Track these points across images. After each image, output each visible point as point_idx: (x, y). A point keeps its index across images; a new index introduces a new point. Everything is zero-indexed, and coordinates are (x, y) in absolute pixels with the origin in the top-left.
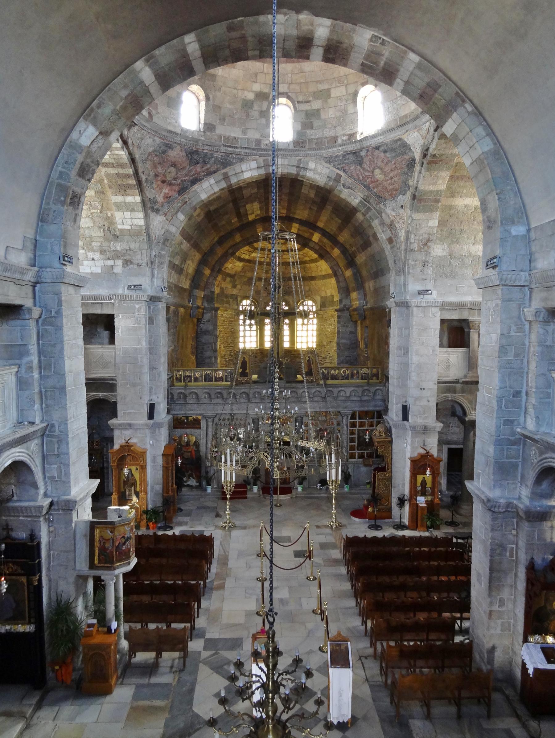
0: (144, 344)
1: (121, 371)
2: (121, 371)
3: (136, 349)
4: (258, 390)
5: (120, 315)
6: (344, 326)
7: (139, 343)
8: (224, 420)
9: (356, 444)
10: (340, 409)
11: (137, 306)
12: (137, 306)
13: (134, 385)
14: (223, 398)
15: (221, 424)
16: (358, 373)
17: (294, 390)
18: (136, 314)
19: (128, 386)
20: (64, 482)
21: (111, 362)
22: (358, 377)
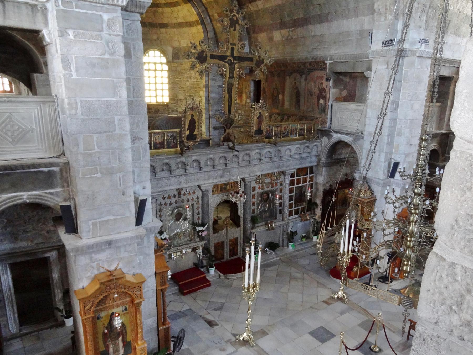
0: (124, 94)
1: (81, 147)
2: (81, 147)
3: (108, 105)
4: (211, 156)
5: (71, 32)
6: (213, 79)
7: (115, 94)
8: (169, 197)
9: (293, 202)
10: (284, 169)
11: (106, 17)
12: (106, 17)
13: (110, 172)
14: (170, 171)
15: (166, 204)
16: (296, 129)
17: (247, 152)
18: (105, 34)
19: (99, 175)
21: (32, 130)
22: (296, 134)
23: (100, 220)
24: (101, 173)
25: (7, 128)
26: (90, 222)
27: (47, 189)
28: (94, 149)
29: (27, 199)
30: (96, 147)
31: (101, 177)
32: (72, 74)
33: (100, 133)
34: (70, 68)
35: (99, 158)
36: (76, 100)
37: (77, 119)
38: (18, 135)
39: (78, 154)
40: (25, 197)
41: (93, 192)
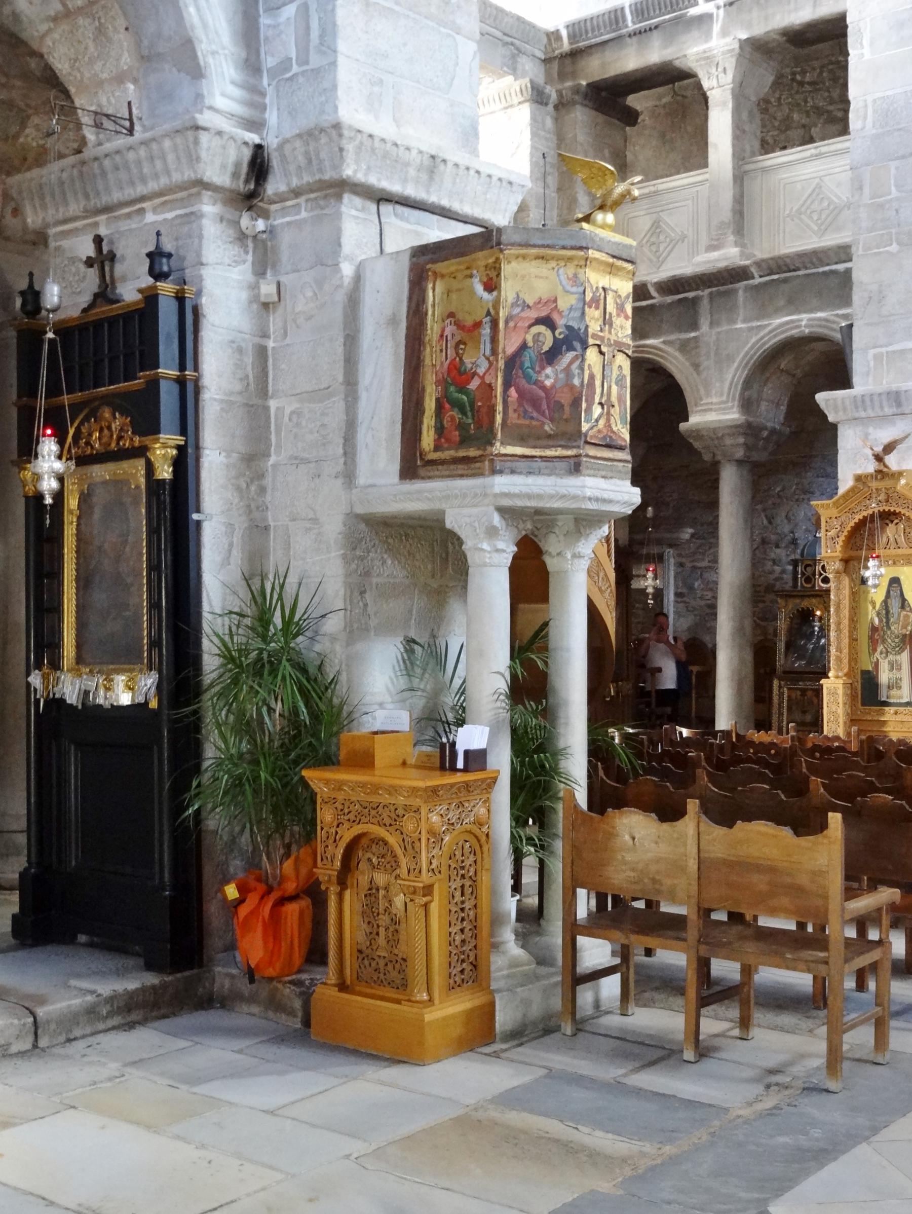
1: (867, 190)
19: (894, 248)
20: (316, 71)
23: (890, 349)
24: (899, 244)
25: (813, 207)
26: (872, 352)
27: (840, 308)
28: (890, 194)
29: (806, 326)
30: (893, 188)
31: (899, 252)
32: (862, 54)
33: (903, 157)
34: (861, 44)
35: (897, 211)
36: (865, 101)
37: (864, 137)
38: (828, 216)
39: (859, 206)
40: (803, 323)
41: (881, 285)
